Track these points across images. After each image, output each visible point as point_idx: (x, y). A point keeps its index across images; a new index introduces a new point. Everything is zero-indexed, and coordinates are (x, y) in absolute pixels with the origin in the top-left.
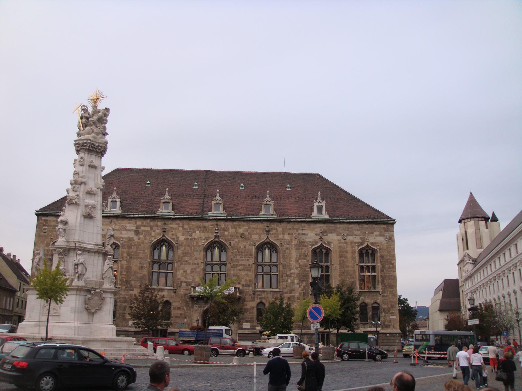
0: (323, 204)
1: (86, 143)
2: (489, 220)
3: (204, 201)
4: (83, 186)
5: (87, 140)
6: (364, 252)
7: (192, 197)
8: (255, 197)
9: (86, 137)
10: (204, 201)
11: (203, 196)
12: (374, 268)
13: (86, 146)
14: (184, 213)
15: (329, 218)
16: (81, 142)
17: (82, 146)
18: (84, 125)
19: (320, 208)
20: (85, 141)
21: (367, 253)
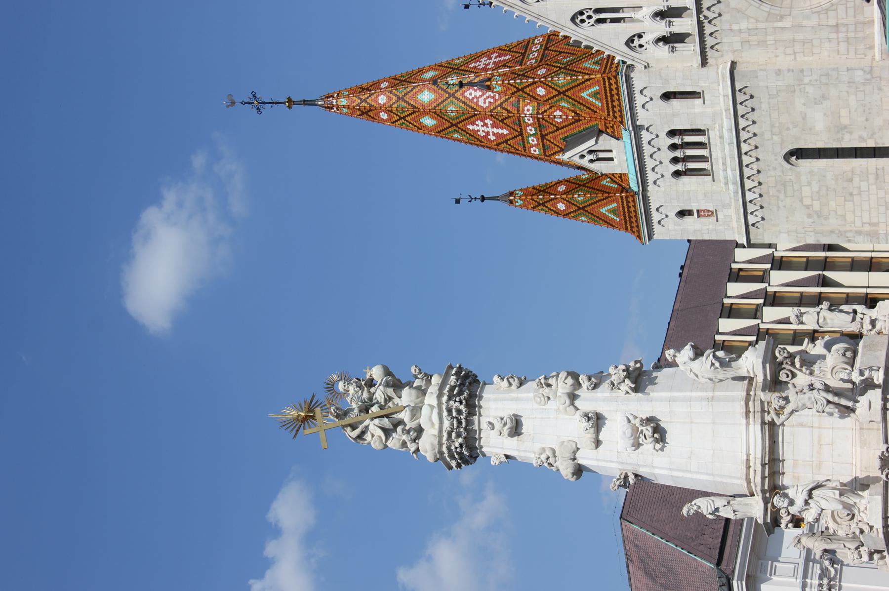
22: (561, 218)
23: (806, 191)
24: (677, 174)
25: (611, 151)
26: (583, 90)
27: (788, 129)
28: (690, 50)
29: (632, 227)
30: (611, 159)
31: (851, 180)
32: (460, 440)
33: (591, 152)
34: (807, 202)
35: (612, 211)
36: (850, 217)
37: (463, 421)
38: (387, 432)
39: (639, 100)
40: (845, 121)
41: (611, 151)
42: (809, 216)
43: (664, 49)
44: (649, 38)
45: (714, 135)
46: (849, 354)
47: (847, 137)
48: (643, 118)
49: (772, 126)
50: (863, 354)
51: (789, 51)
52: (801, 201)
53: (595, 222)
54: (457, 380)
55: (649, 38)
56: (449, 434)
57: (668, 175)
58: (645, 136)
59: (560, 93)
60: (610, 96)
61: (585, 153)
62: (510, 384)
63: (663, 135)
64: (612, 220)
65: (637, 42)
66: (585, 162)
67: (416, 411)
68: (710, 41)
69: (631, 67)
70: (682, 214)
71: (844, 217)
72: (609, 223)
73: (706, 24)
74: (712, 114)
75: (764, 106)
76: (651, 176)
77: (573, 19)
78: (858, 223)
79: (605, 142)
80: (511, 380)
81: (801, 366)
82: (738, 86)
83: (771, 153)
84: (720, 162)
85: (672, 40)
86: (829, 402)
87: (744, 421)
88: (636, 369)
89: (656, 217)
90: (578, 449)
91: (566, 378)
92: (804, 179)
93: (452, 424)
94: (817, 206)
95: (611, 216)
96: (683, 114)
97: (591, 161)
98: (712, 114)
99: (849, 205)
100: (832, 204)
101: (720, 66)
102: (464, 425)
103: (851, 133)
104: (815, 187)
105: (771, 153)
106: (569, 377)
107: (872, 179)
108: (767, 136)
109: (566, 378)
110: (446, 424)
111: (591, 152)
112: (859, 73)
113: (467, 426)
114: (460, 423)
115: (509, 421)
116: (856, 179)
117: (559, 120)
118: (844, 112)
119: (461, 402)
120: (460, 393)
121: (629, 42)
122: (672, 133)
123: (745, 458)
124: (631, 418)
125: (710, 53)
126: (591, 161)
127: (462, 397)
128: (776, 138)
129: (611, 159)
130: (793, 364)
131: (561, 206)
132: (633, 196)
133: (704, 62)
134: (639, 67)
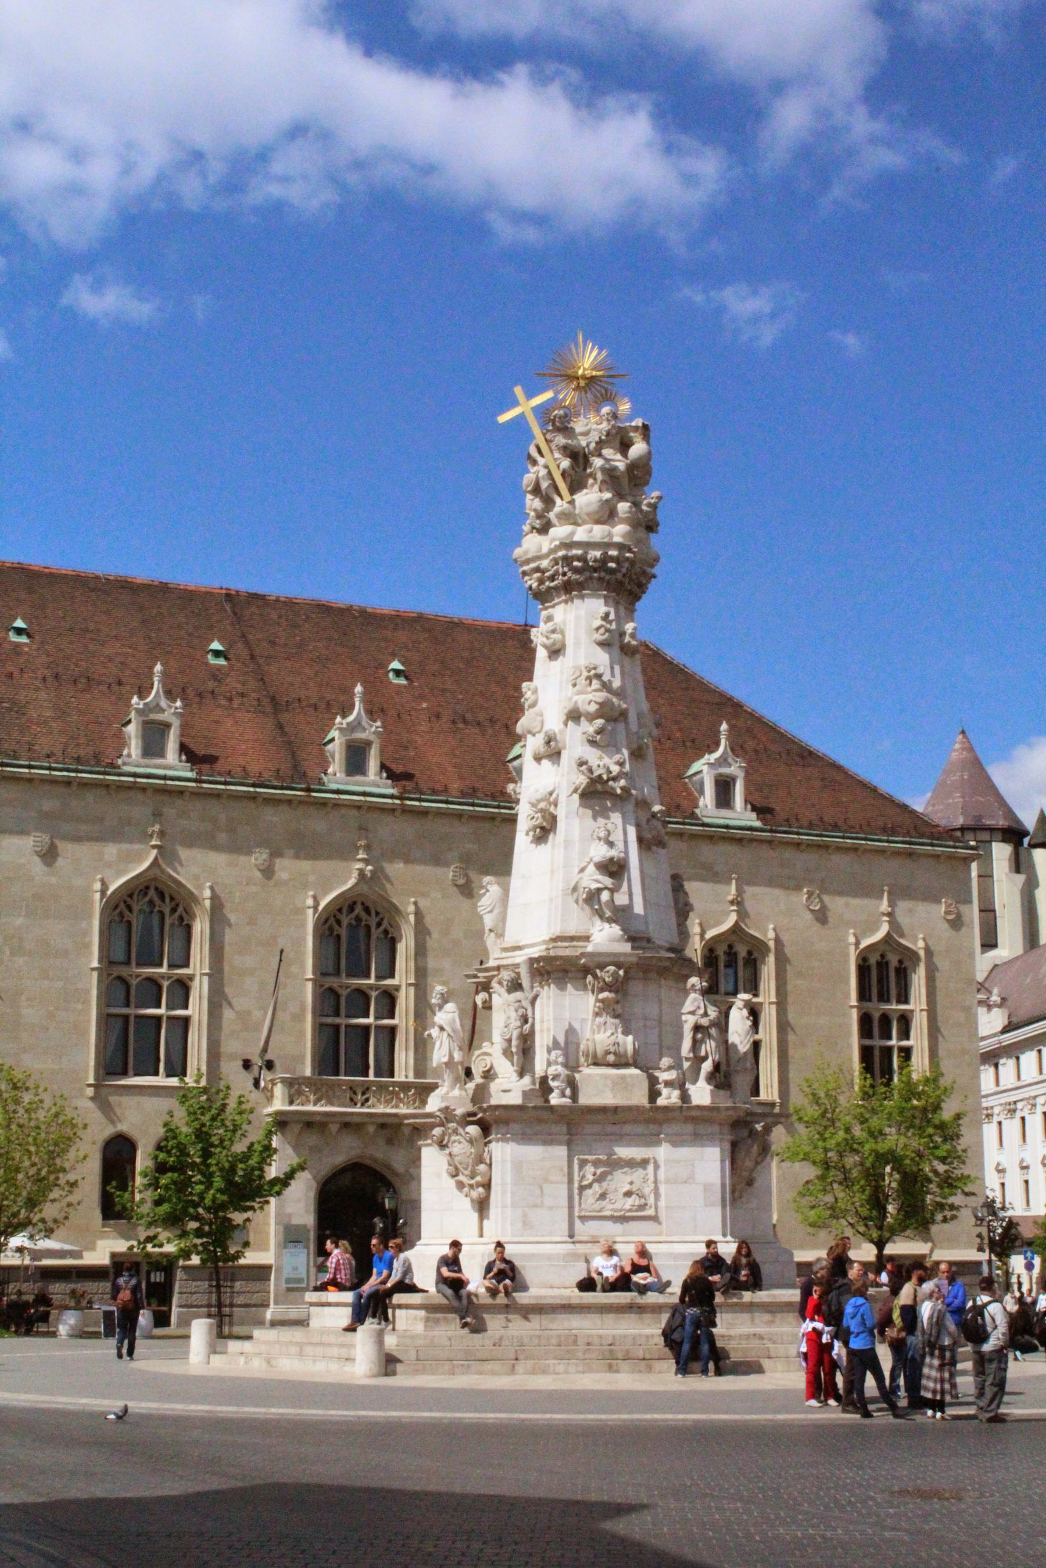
0: (735, 769)
1: (612, 559)
2: (1026, 841)
3: (281, 727)
4: (621, 726)
5: (620, 547)
6: (721, 951)
7: (223, 702)
8: (465, 722)
9: (598, 532)
10: (281, 727)
11: (266, 701)
12: (905, 1021)
13: (612, 571)
14: (229, 773)
15: (758, 824)
16: (598, 554)
17: (595, 570)
18: (569, 480)
19: (724, 788)
20: (613, 553)
21: (883, 965)
32: (535, 585)
37: (555, 583)
38: (536, 490)
46: (611, 1058)
50: (606, 1077)
54: (595, 561)
56: (537, 570)
62: (597, 629)
67: (570, 518)
80: (602, 630)
81: (603, 1001)
86: (509, 1041)
87: (547, 938)
88: (613, 789)
90: (534, 735)
91: (596, 703)
93: (548, 571)
102: (552, 584)
106: (597, 707)
109: (596, 703)
110: (545, 563)
113: (552, 588)
114: (552, 578)
115: (552, 641)
119: (564, 574)
120: (576, 570)
123: (521, 944)
124: (554, 795)
127: (569, 574)
130: (602, 990)
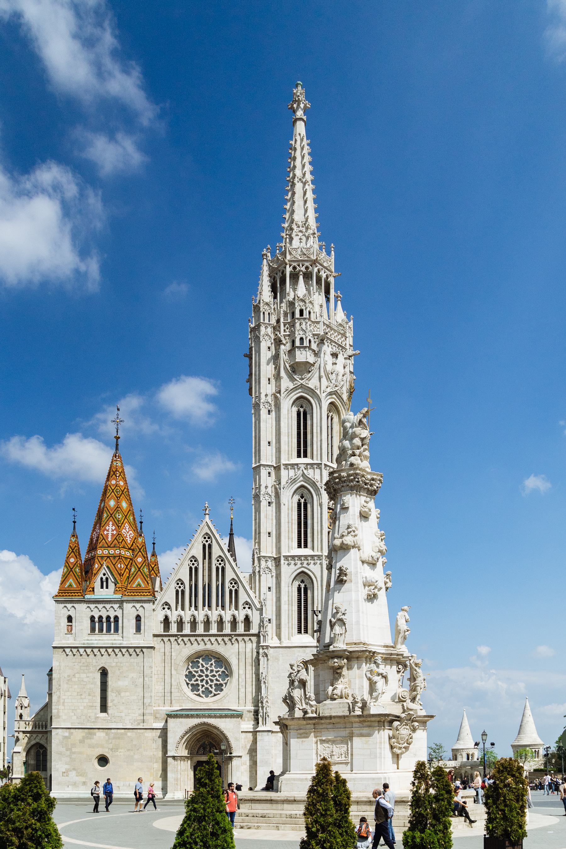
22: (65, 559)
23: (85, 675)
24: (92, 618)
25: (107, 588)
26: (141, 579)
27: (119, 670)
28: (160, 630)
29: (62, 593)
30: (102, 587)
31: (89, 695)
33: (107, 579)
34: (77, 675)
35: (70, 585)
36: (69, 694)
39: (138, 605)
40: (123, 694)
41: (107, 588)
42: (69, 676)
43: (162, 618)
44: (168, 613)
45: (115, 637)
47: (114, 695)
48: (127, 607)
49: (121, 663)
51: (159, 672)
52: (78, 673)
53: (63, 576)
55: (168, 613)
57: (93, 614)
58: (116, 606)
59: (139, 569)
60: (139, 591)
61: (107, 576)
63: (116, 613)
64: (65, 584)
65: (166, 607)
66: (101, 575)
68: (166, 639)
69: (154, 603)
70: (70, 619)
71: (68, 691)
72: (62, 583)
73: (175, 638)
74: (128, 636)
75: (132, 660)
76: (92, 606)
77: (180, 580)
78: (64, 697)
79: (112, 586)
82: (144, 650)
83: (104, 661)
84: (100, 638)
85: (166, 621)
89: (69, 606)
92: (91, 675)
94: (74, 679)
95: (68, 584)
96: (129, 624)
97: (102, 578)
98: (128, 636)
99: (75, 694)
100: (76, 686)
101: (151, 642)
103: (116, 696)
104: (85, 680)
105: (104, 661)
107: (91, 704)
108: (115, 660)
111: (107, 579)
112: (149, 701)
116: (90, 697)
117: (119, 566)
118: (128, 694)
121: (166, 603)
122: (116, 618)
125: (160, 639)
126: (102, 578)
128: (114, 664)
129: (102, 587)
131: (72, 560)
132: (82, 595)
133: (155, 636)
134: (154, 607)
